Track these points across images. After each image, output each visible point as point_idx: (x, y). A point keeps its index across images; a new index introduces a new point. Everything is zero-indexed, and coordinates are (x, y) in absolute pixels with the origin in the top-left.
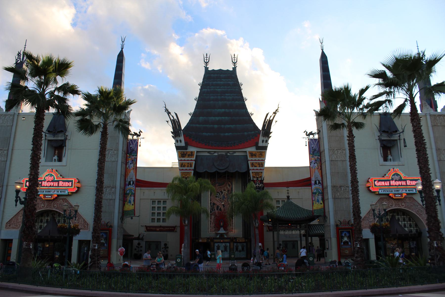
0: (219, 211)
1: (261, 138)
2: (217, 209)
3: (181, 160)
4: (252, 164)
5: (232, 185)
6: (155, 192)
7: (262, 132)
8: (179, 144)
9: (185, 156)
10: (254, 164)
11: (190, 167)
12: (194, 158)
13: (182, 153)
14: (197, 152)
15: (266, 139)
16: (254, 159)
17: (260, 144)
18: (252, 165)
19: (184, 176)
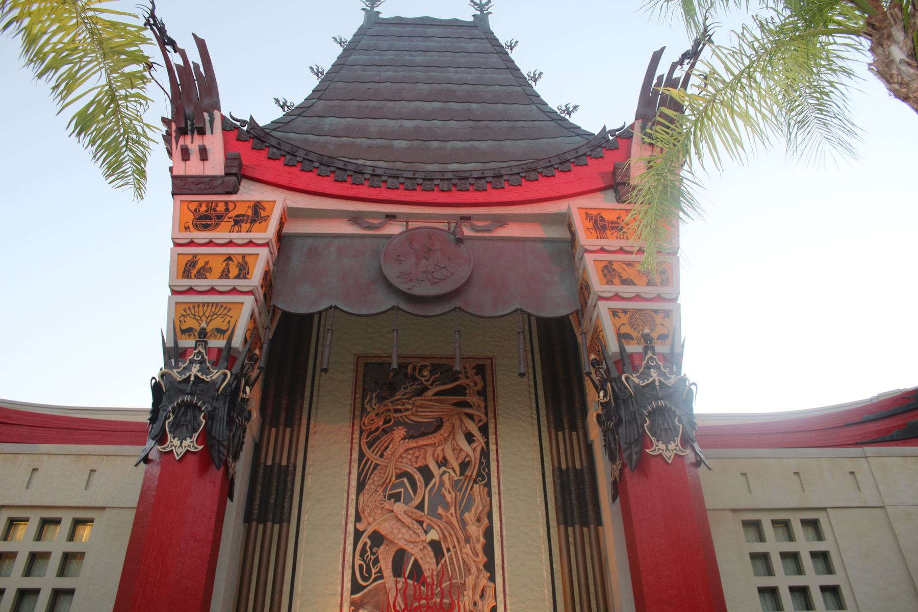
0: (410, 582)
2: (397, 571)
4: (606, 267)
6: (35, 470)
8: (194, 167)
9: (217, 225)
10: (614, 267)
11: (238, 277)
12: (265, 231)
13: (203, 208)
16: (612, 243)
18: (608, 272)
19: (190, 323)
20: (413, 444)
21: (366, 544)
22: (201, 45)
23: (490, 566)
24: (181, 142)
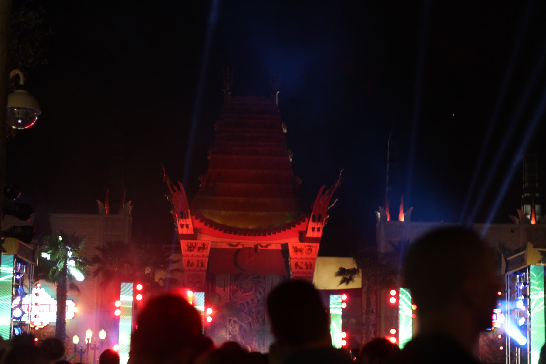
9: (193, 250)
10: (299, 264)
13: (189, 244)
15: (318, 226)
20: (244, 295)
21: (232, 323)
24: (180, 223)
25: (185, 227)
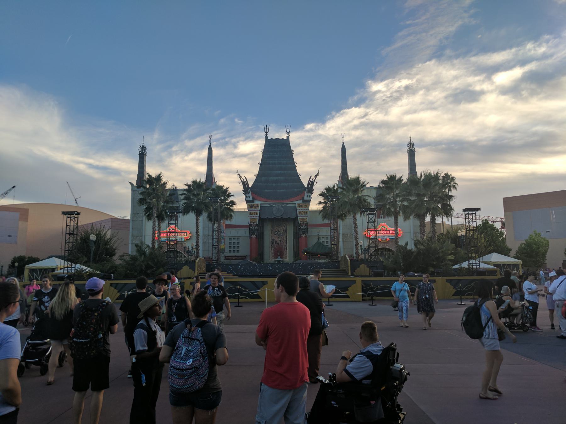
1: (306, 194)
2: (276, 243)
3: (250, 210)
5: (286, 226)
7: (306, 189)
8: (248, 199)
10: (301, 212)
14: (261, 204)
17: (306, 198)
18: (300, 212)
19: (252, 221)
22: (245, 178)
23: (286, 243)
25: (248, 197)
